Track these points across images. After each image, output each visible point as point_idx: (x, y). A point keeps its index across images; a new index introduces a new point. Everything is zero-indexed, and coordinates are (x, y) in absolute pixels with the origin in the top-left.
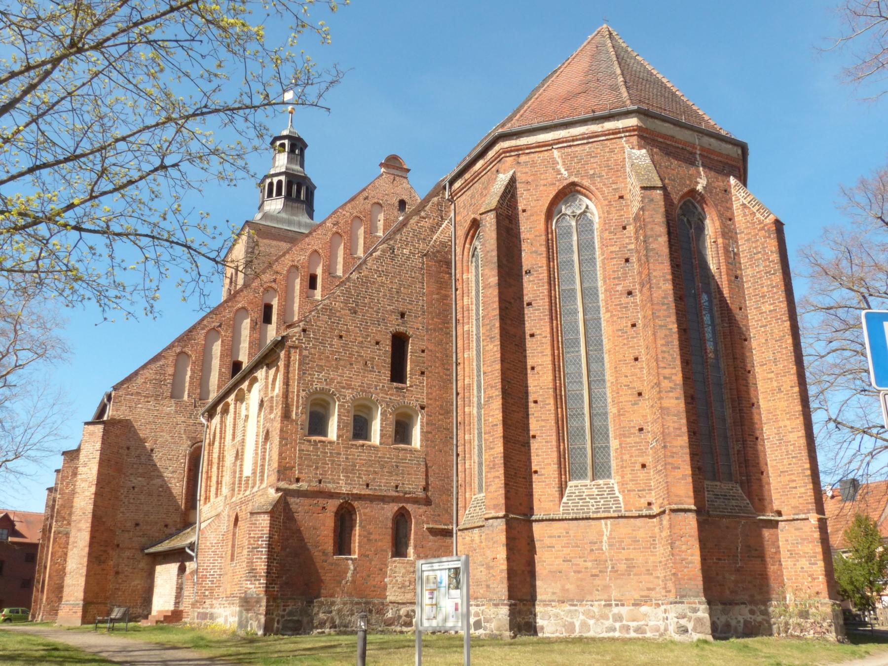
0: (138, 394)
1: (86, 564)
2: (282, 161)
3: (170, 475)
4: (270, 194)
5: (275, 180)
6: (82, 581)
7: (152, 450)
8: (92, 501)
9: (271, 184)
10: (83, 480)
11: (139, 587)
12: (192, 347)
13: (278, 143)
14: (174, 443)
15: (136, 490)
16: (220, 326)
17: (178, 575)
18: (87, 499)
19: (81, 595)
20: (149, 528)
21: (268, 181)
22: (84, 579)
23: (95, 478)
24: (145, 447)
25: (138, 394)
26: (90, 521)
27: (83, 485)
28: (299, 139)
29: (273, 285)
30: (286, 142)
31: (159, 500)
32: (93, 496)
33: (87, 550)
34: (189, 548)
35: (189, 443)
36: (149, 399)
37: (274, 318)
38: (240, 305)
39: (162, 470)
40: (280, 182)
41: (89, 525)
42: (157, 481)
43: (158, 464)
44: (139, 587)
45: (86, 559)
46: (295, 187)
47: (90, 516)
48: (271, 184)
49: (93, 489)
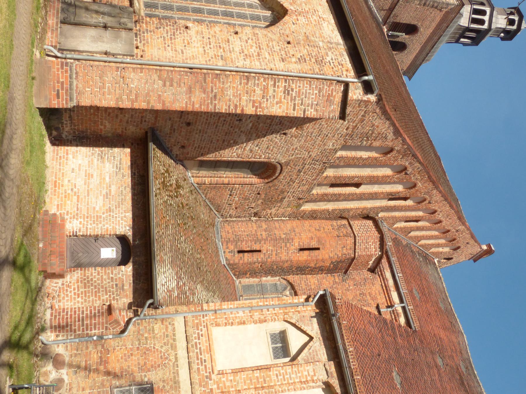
0: (362, 121)
1: (136, 106)
2: (500, 22)
3: (248, 148)
4: (476, 12)
5: (486, 18)
6: (108, 101)
7: (285, 134)
8: (232, 110)
9: (483, 13)
10: (265, 89)
11: (102, 127)
12: (394, 157)
13: (516, 18)
14: (288, 150)
15: (237, 123)
16: (406, 174)
17: (116, 235)
18: (236, 100)
19: (86, 102)
20: (183, 133)
21: (488, 10)
22: (112, 104)
23: (266, 112)
24: (291, 128)
25: (362, 121)
26: (204, 109)
27: (258, 91)
28: (511, 39)
29: (427, 202)
30: (515, 27)
31: (218, 140)
32: (239, 111)
33: (159, 107)
34: (152, 304)
35: (283, 161)
36: (350, 129)
37: (392, 203)
38: (419, 184)
39: (256, 142)
40: (482, 22)
41: (197, 107)
42: (243, 137)
43: (265, 139)
44: (102, 127)
45: (144, 105)
46: (473, 35)
47: (211, 108)
48: (483, 13)
49: (250, 110)
